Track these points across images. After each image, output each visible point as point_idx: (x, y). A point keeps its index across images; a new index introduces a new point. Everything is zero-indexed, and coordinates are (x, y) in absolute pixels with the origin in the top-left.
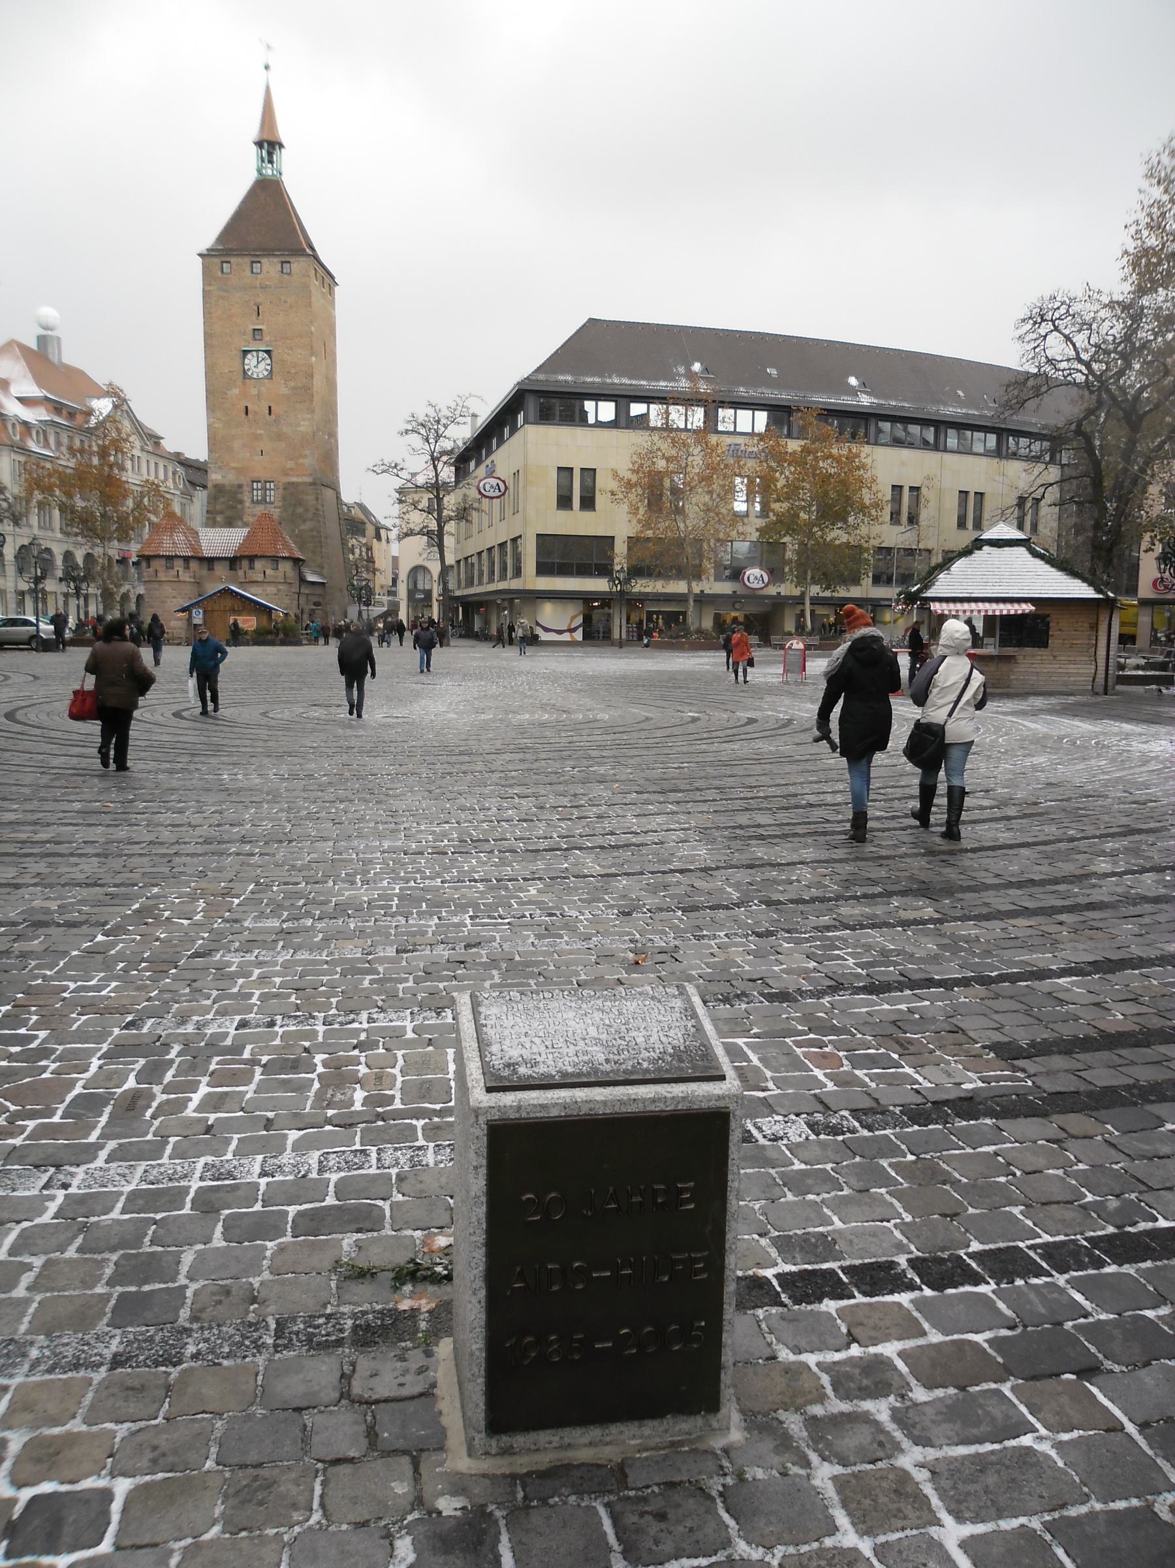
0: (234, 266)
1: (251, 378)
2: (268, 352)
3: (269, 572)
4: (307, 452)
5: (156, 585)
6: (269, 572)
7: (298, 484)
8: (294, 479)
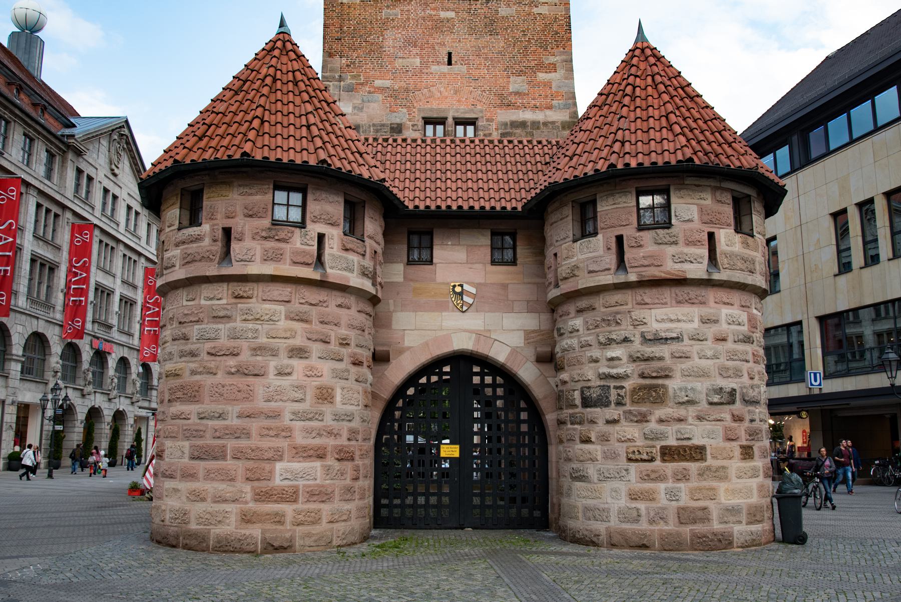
3: (727, 238)
4: (552, 59)
5: (219, 297)
6: (727, 238)
7: (536, 125)
8: (528, 116)
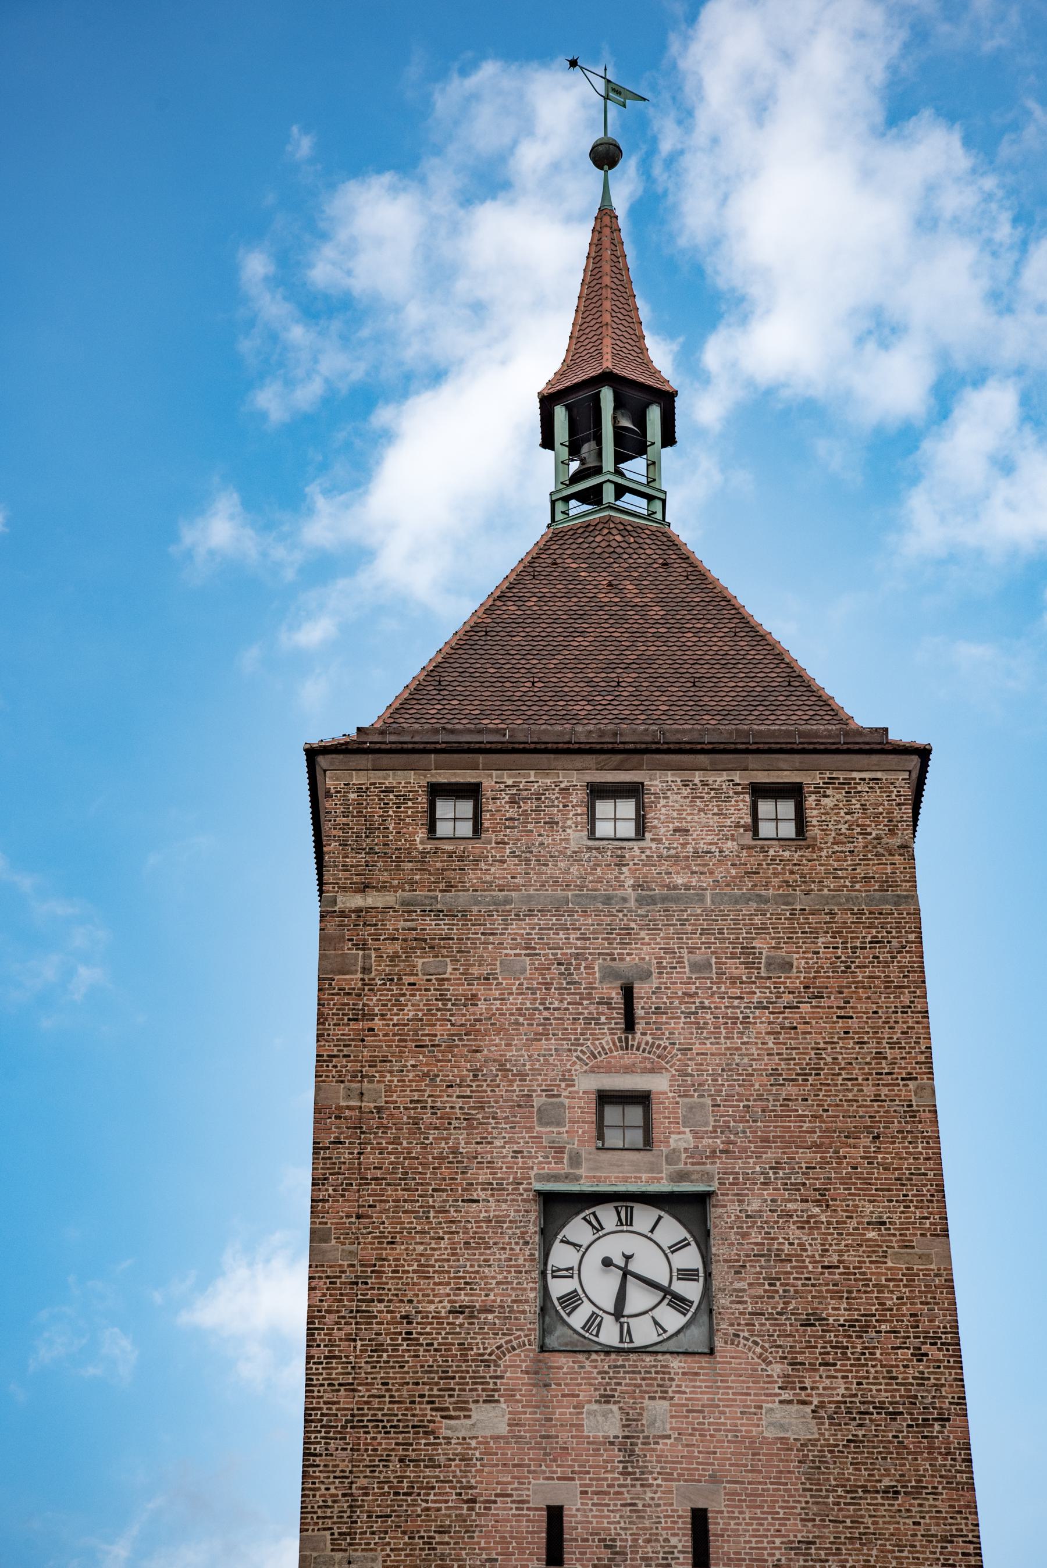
0: (498, 807)
1: (585, 1347)
2: (691, 1207)
